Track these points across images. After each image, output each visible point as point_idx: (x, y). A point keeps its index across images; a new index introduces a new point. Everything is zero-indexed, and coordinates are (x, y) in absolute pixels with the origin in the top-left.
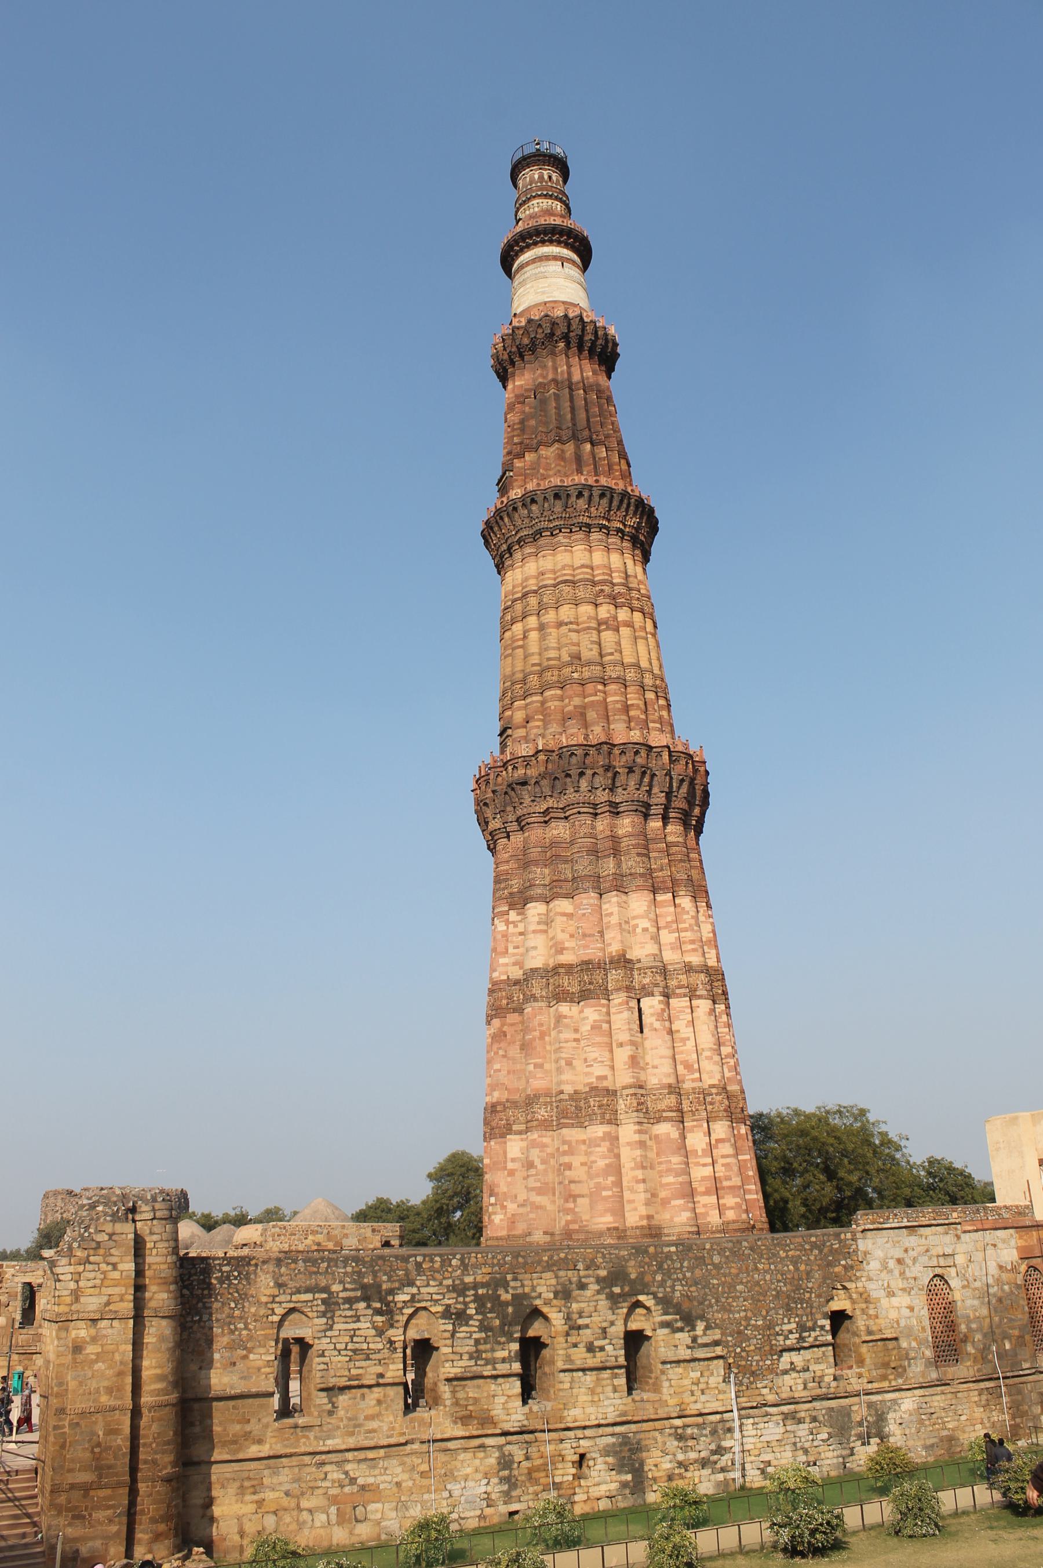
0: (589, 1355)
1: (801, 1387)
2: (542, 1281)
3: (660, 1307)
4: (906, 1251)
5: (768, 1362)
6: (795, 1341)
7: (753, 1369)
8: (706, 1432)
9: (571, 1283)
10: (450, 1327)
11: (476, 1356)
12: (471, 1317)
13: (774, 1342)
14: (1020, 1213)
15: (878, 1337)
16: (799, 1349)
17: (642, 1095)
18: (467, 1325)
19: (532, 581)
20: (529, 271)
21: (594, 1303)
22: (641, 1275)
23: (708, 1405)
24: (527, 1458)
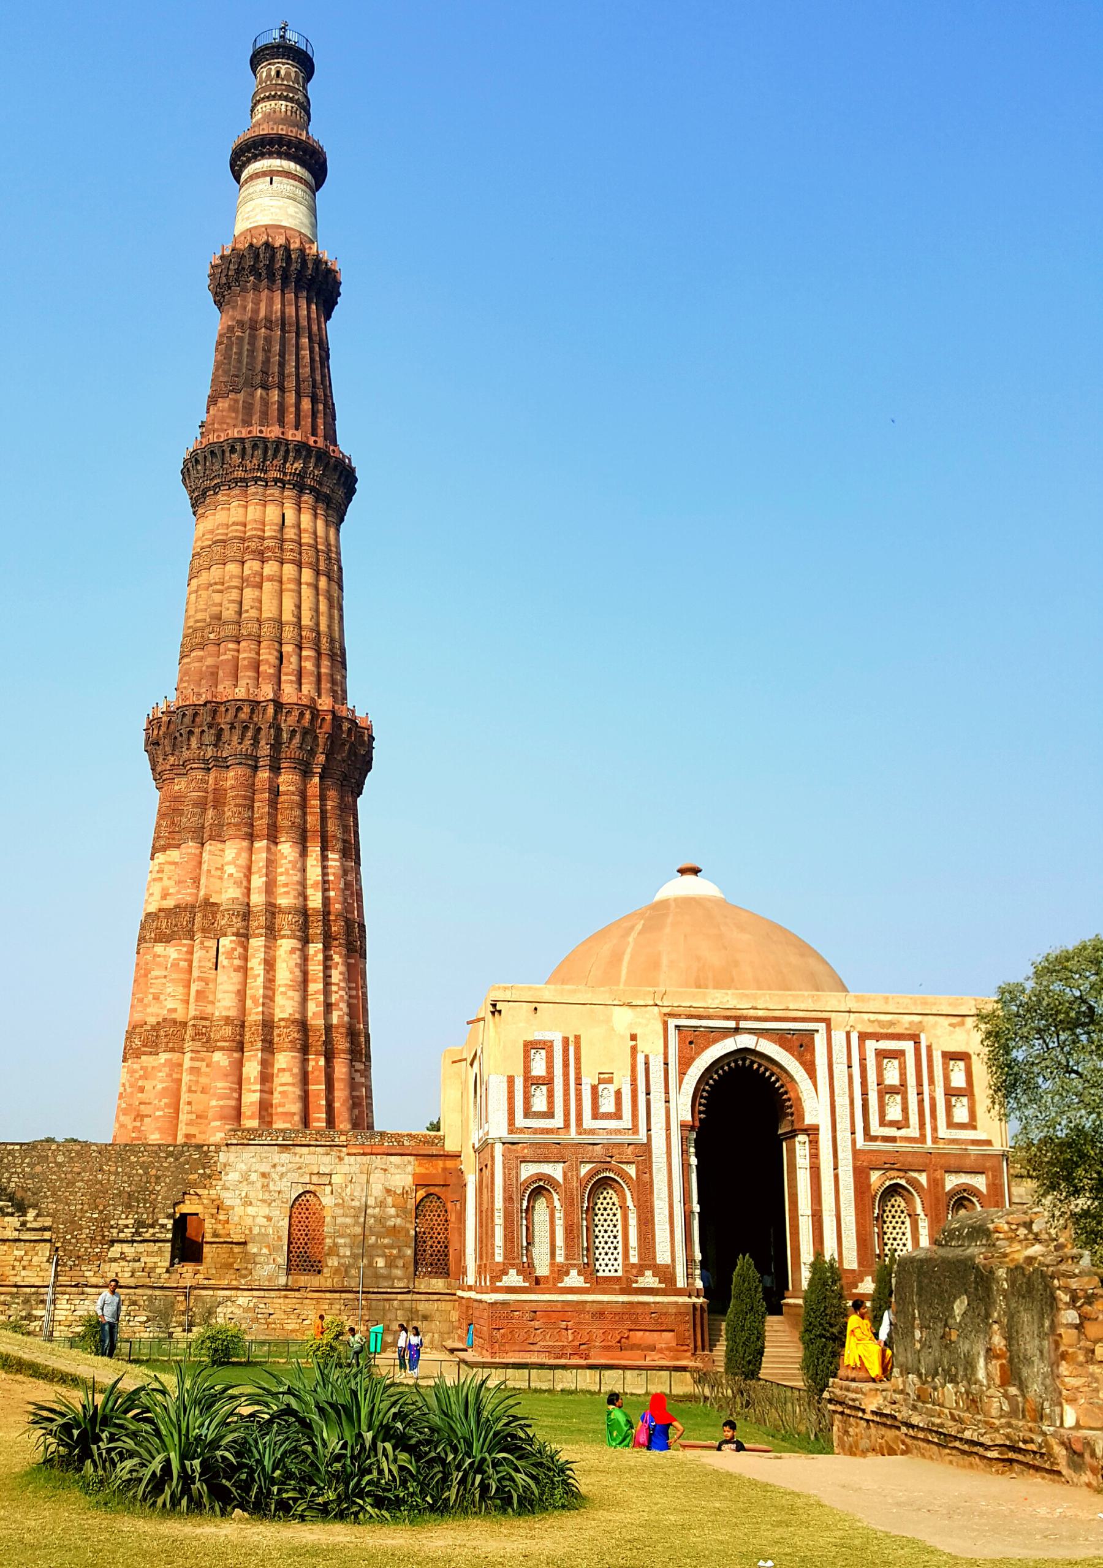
4: (274, 1166)
14: (428, 1142)
15: (222, 1240)
16: (133, 1241)
23: (26, 1279)
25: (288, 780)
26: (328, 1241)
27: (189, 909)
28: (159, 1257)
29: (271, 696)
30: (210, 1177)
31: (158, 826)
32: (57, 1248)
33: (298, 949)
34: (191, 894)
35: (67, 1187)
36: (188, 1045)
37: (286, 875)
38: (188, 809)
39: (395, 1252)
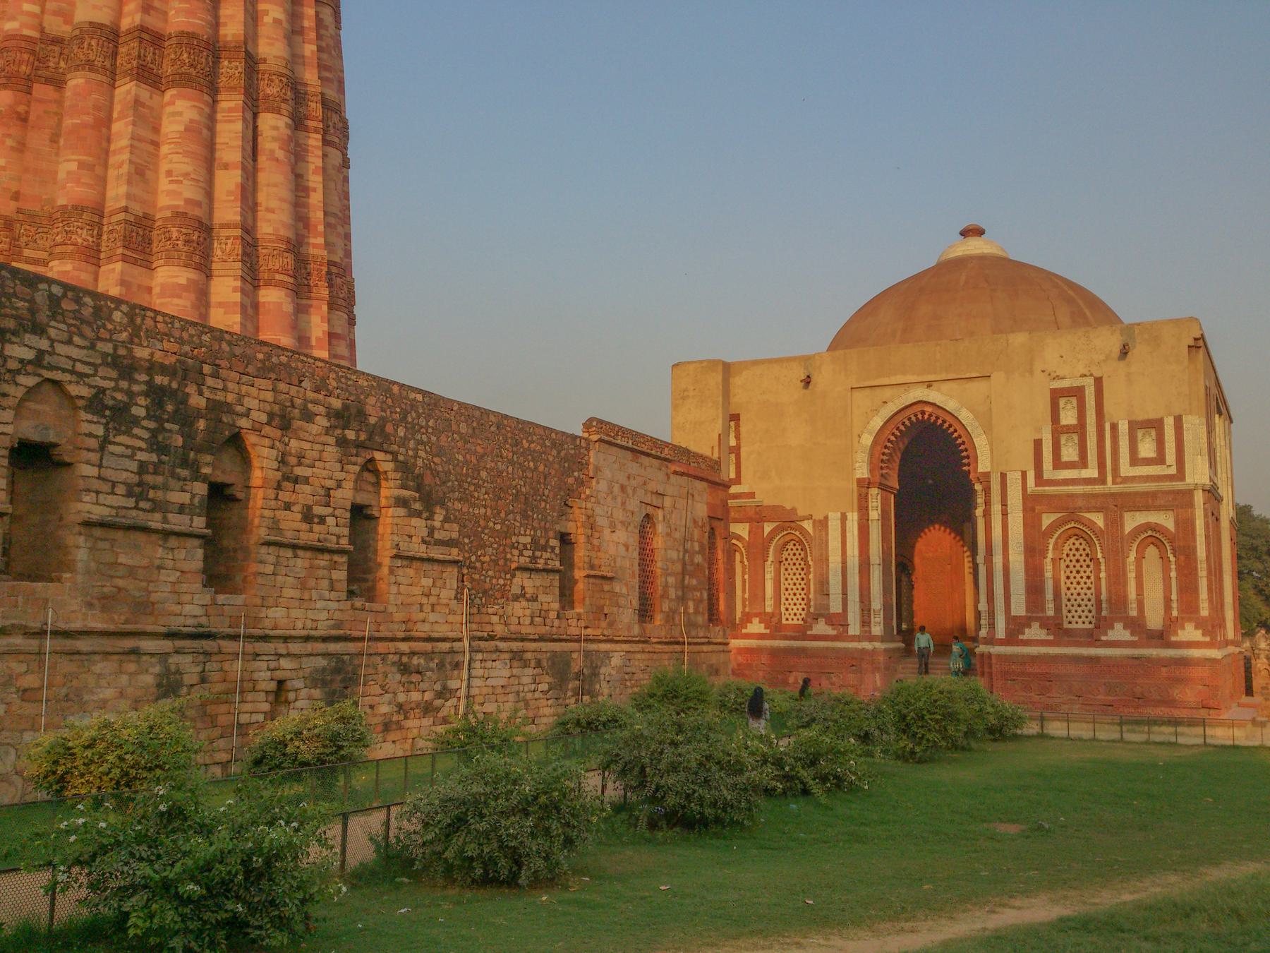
0: (304, 526)
1: (528, 621)
2: (253, 391)
3: (399, 475)
5: (501, 582)
7: (487, 586)
8: (433, 665)
9: (293, 406)
10: (100, 431)
11: (137, 491)
12: (136, 421)
13: (509, 556)
18: (127, 432)
22: (384, 421)
23: (436, 627)
24: (203, 680)
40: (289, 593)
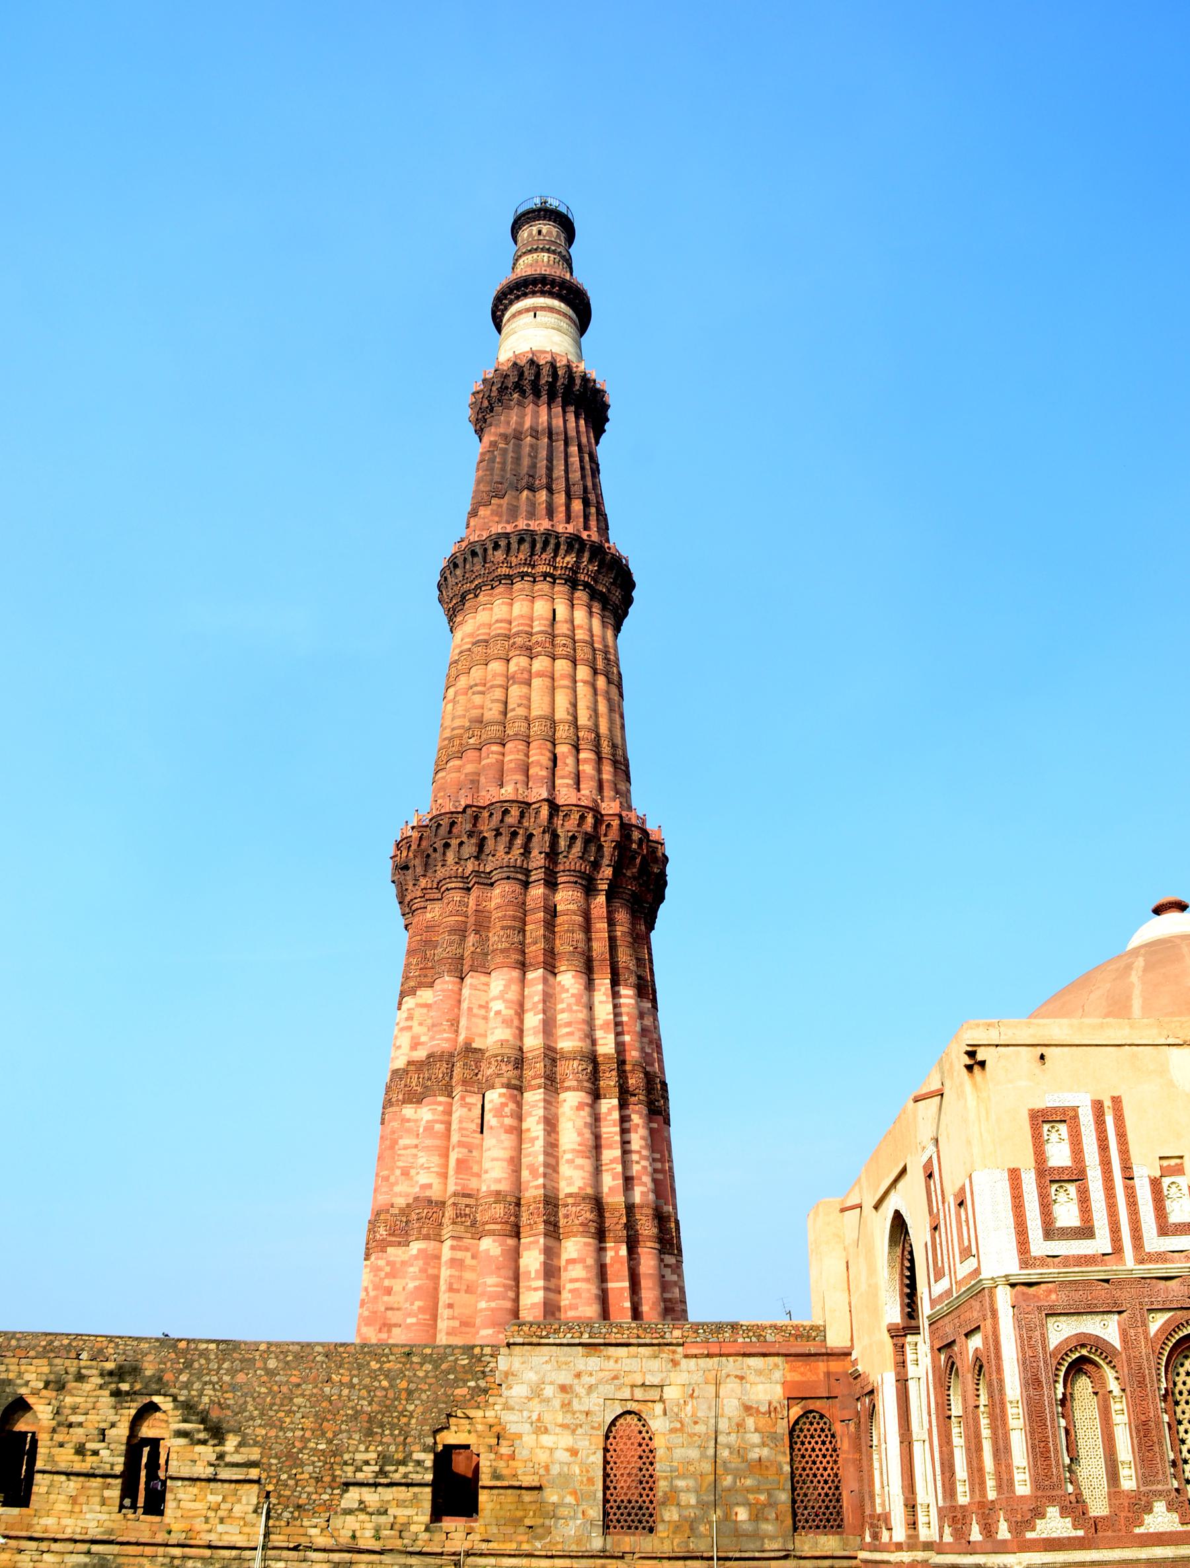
0: (77, 1458)
1: (369, 1533)
2: (32, 1368)
4: (578, 1375)
6: (371, 1475)
7: (301, 1502)
9: (67, 1373)
13: (338, 1473)
14: (801, 1336)
15: (506, 1483)
16: (376, 1485)
17: (467, 1206)
19: (457, 651)
20: (504, 331)
21: (94, 1400)
23: (225, 1537)
25: (567, 898)
26: (662, 1485)
27: (448, 1059)
28: (415, 1510)
29: (545, 795)
30: (485, 1391)
31: (407, 965)
32: (268, 1493)
33: (587, 1105)
34: (447, 1040)
35: (282, 1405)
36: (446, 1232)
37: (568, 1013)
38: (444, 938)
39: (763, 1498)
40: (60, 1506)
